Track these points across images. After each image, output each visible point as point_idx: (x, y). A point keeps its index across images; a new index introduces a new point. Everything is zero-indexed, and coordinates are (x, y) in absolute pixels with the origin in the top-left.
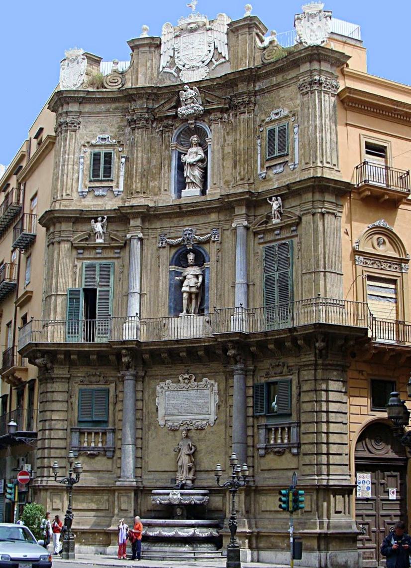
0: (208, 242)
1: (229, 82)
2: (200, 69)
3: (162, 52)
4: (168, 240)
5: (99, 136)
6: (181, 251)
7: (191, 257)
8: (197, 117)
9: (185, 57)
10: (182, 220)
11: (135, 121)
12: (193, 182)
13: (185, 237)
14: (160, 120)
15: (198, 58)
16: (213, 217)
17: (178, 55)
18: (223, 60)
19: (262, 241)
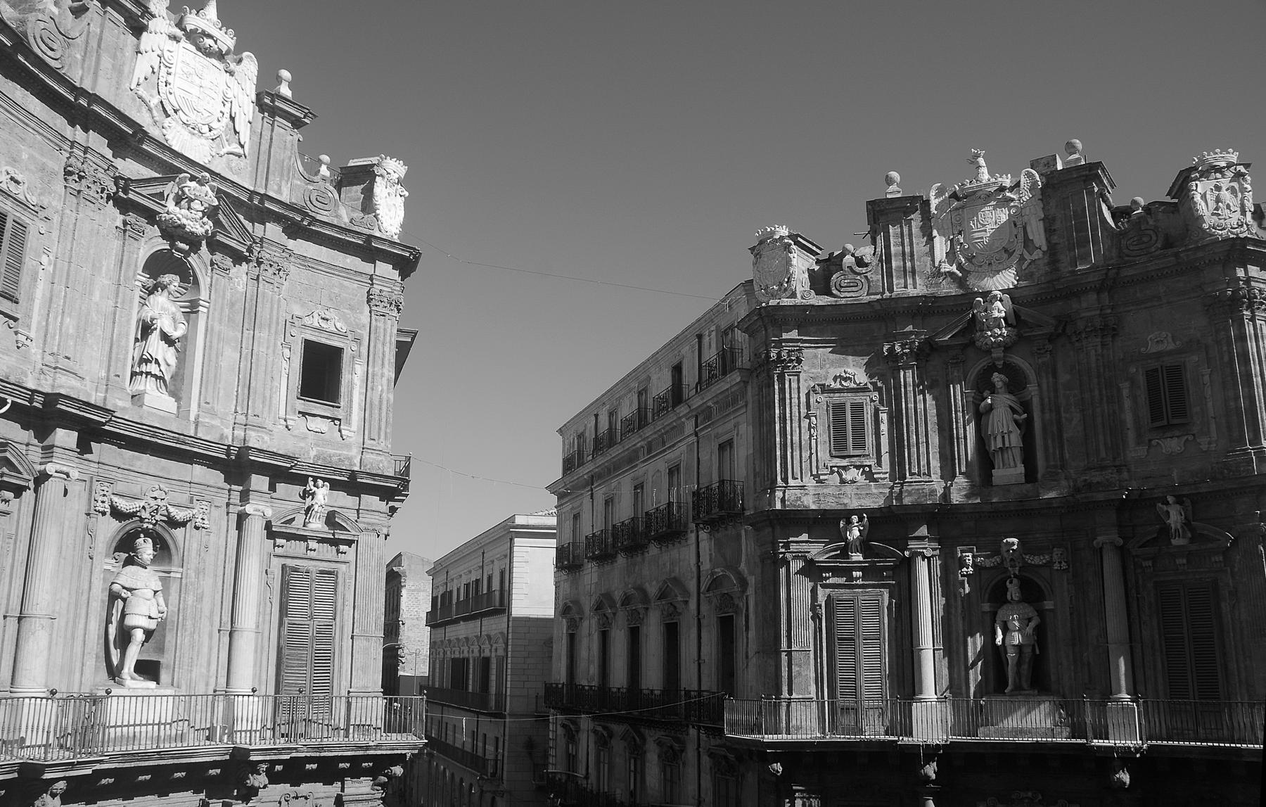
0: (183, 524)
1: (258, 209)
2: (203, 141)
3: (142, 48)
4: (115, 499)
5: (9, 169)
6: (128, 528)
7: (146, 549)
8: (194, 242)
9: (183, 94)
10: (139, 459)
11: (81, 178)
12: (161, 378)
13: (153, 503)
14: (124, 206)
15: (206, 114)
16: (198, 472)
17: (170, 79)
18: (240, 151)
19: (279, 551)
